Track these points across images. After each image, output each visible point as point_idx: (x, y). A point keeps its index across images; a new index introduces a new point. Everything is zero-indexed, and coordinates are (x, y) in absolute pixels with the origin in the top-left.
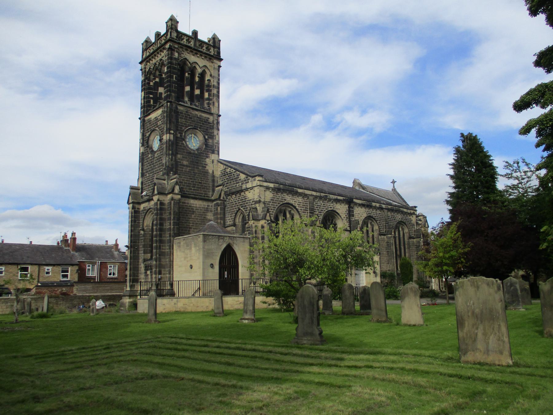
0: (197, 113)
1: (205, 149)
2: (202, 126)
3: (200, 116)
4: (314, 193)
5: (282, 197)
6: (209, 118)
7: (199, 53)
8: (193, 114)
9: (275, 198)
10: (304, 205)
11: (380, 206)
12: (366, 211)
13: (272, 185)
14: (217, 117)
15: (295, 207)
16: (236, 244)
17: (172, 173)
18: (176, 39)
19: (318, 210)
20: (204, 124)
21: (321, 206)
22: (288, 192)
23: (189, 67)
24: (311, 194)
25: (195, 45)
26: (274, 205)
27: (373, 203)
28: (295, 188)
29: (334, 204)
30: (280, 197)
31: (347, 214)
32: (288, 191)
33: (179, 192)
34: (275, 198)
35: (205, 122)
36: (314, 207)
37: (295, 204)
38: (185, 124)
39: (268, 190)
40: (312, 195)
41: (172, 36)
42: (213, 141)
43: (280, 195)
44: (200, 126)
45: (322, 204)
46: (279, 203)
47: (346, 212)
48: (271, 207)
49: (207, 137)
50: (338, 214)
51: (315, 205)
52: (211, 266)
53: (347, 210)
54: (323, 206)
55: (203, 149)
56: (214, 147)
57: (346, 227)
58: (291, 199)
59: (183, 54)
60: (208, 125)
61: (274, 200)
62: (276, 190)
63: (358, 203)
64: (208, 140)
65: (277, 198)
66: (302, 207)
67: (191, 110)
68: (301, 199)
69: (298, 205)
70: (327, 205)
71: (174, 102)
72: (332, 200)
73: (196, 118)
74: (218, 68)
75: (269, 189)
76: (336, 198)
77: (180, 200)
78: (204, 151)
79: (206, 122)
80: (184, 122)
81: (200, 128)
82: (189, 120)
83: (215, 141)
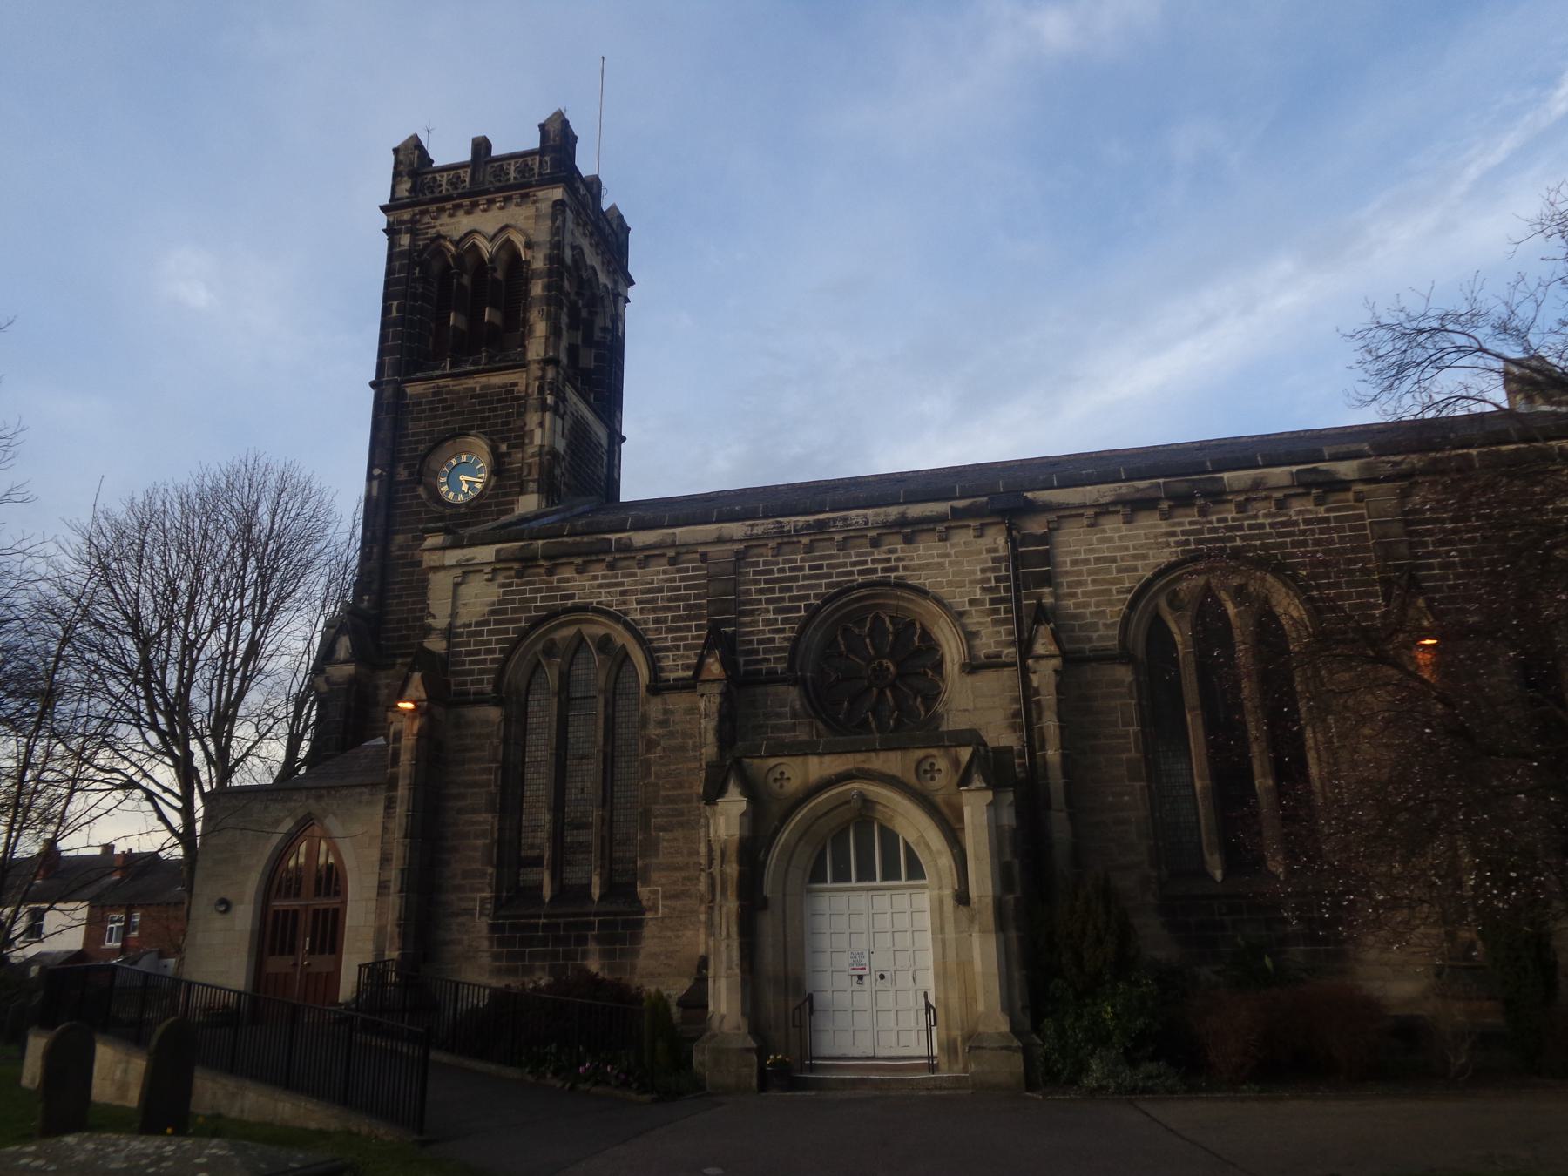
0: (470, 383)
1: (494, 488)
2: (489, 418)
3: (481, 389)
4: (736, 529)
5: (549, 590)
6: (515, 384)
7: (482, 199)
8: (458, 392)
9: (513, 602)
10: (678, 598)
11: (1309, 478)
12: (1173, 534)
13: (486, 553)
14: (543, 370)
15: (617, 618)
16: (335, 815)
17: (366, 598)
18: (407, 198)
19: (768, 601)
20: (495, 409)
21: (795, 579)
22: (578, 561)
23: (453, 256)
24: (714, 536)
25: (470, 184)
26: (507, 631)
27: (1226, 475)
28: (614, 537)
29: (890, 551)
30: (540, 590)
31: (998, 580)
32: (579, 555)
33: (353, 655)
34: (513, 602)
35: (499, 401)
36: (748, 592)
37: (624, 602)
38: (427, 433)
39: (471, 576)
40: (720, 540)
41: (398, 195)
42: (523, 451)
43: (542, 582)
44: (483, 419)
45: (801, 568)
46: (527, 620)
47: (993, 570)
48: (489, 642)
49: (504, 448)
50: (921, 592)
51: (756, 582)
52: (222, 908)
53: (995, 560)
54: (805, 578)
55: (488, 492)
56: (525, 473)
57: (993, 649)
58: (600, 586)
59: (434, 227)
60: (511, 407)
61: (504, 612)
62: (516, 566)
63: (1084, 506)
64: (508, 454)
65: (521, 601)
66: (669, 609)
67: (451, 383)
68: (665, 572)
69: (639, 602)
70: (845, 565)
71: (388, 382)
72: (873, 533)
73: (465, 403)
74: (550, 210)
75: (482, 571)
76: (892, 518)
77: (353, 680)
78: (490, 497)
79: (505, 400)
80: (425, 427)
81: (479, 427)
82: (442, 416)
83: (531, 450)
